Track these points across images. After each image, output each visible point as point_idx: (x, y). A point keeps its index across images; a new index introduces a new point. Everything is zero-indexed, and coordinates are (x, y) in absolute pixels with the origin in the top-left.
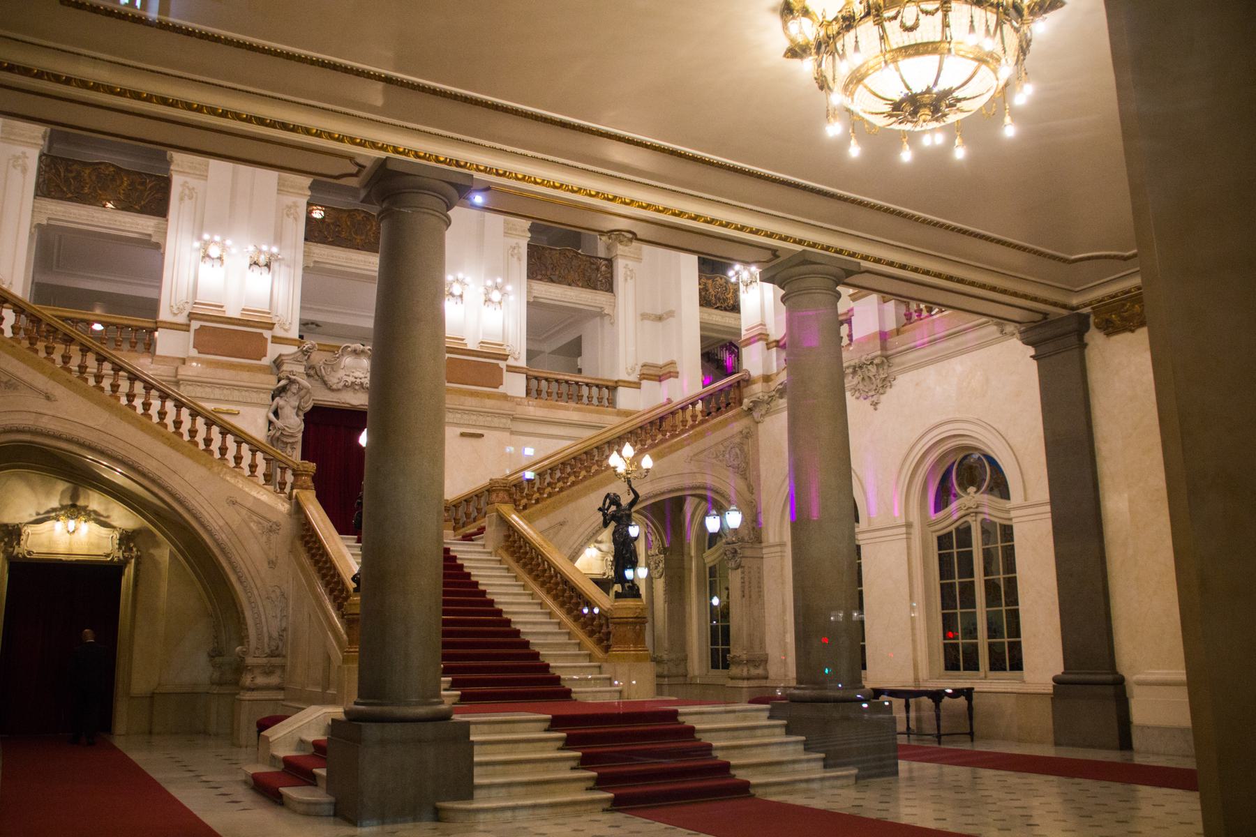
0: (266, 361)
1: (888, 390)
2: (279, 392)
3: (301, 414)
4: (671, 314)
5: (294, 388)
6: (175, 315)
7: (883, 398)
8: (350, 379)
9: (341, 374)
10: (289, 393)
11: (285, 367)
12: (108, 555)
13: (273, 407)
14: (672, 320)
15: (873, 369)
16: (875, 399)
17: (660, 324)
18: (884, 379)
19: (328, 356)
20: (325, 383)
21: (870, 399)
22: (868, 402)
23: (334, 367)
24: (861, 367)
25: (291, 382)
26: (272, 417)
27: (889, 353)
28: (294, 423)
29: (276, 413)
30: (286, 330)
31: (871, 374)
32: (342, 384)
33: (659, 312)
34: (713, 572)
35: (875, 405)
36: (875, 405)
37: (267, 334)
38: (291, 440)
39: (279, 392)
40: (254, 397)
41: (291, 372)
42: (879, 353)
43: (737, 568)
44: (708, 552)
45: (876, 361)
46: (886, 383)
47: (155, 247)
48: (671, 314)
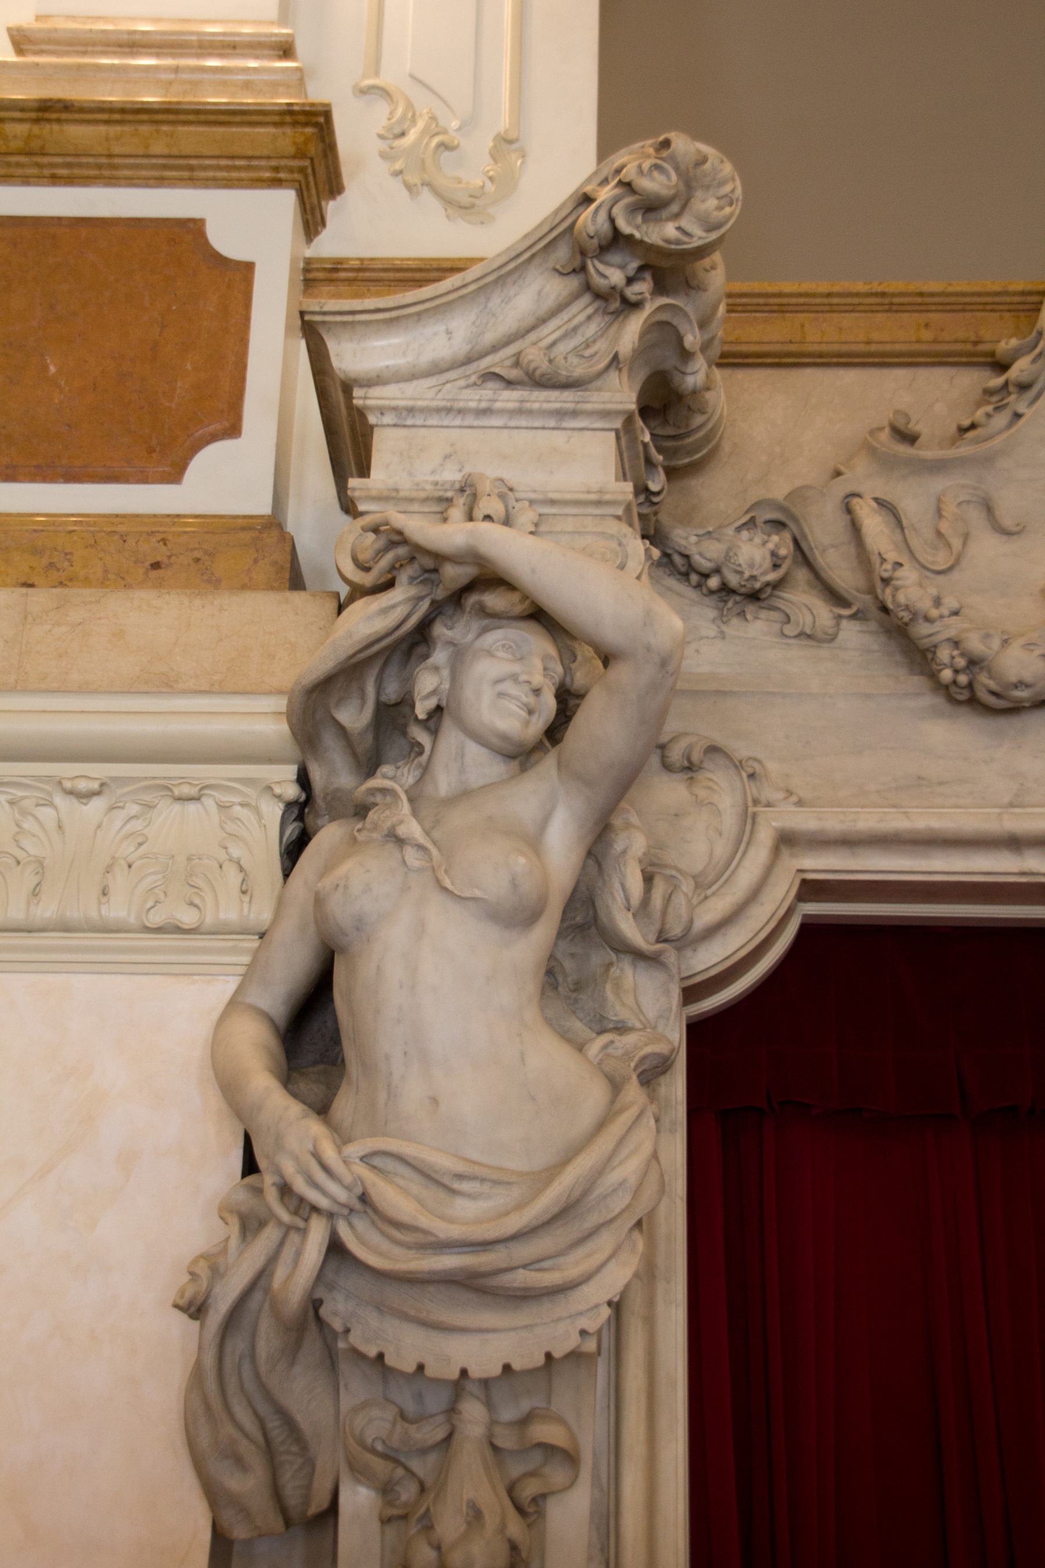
0: (224, 480)
3: (654, 1014)
5: (497, 679)
10: (458, 761)
19: (937, 396)
25: (473, 588)
26: (253, 1045)
30: (464, 207)
37: (250, 224)
38: (488, 1342)
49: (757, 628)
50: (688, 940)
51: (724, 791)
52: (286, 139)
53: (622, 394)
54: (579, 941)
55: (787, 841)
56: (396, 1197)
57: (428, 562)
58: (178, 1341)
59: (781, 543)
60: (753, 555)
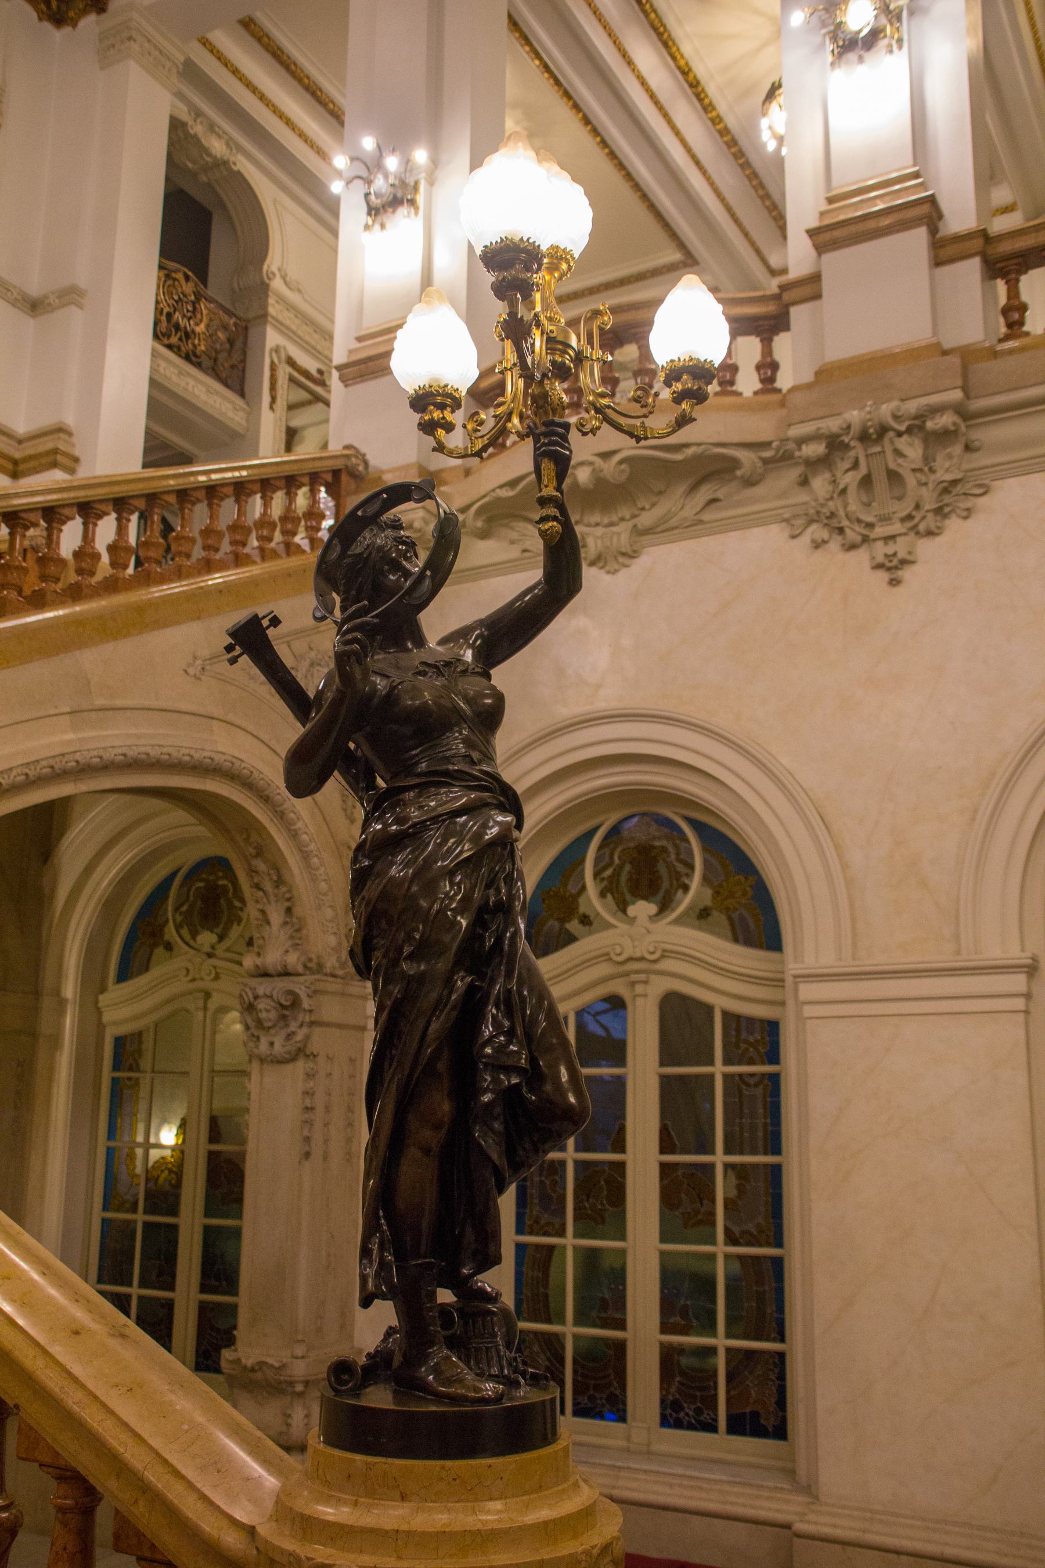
1: (953, 524)
4: (70, 295)
7: (925, 548)
14: (75, 318)
15: (913, 450)
16: (900, 548)
17: (30, 324)
18: (947, 488)
21: (881, 550)
22: (861, 557)
24: (864, 437)
27: (978, 404)
31: (904, 469)
33: (34, 288)
34: (127, 1051)
35: (893, 568)
36: (893, 568)
42: (957, 395)
43: (292, 1059)
44: (116, 992)
45: (946, 420)
46: (952, 499)
48: (70, 295)
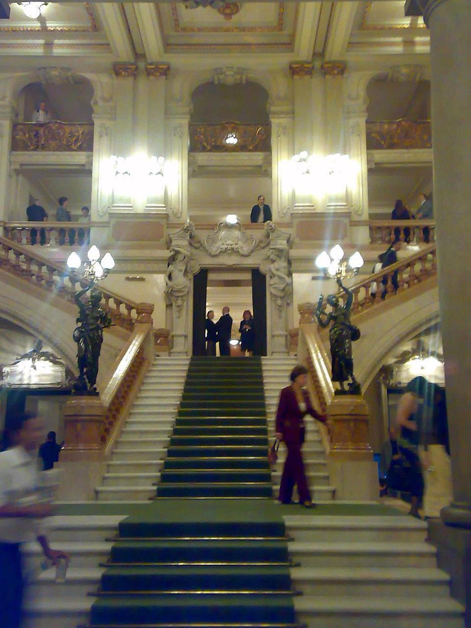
2: (172, 260)
3: (191, 276)
5: (180, 257)
6: (101, 216)
8: (225, 247)
9: (219, 244)
10: (177, 261)
11: (174, 243)
12: (59, 383)
13: (168, 273)
20: (207, 251)
23: (214, 241)
25: (177, 252)
26: (167, 279)
28: (184, 283)
29: (170, 277)
32: (219, 251)
38: (182, 294)
39: (172, 260)
40: (156, 267)
41: (177, 246)
47: (86, 171)
49: (198, 250)
50: (193, 271)
51: (195, 261)
52: (165, 216)
53: (188, 237)
54: (186, 273)
55: (199, 265)
56: (175, 287)
57: (176, 251)
58: (164, 295)
59: (199, 244)
60: (197, 245)
